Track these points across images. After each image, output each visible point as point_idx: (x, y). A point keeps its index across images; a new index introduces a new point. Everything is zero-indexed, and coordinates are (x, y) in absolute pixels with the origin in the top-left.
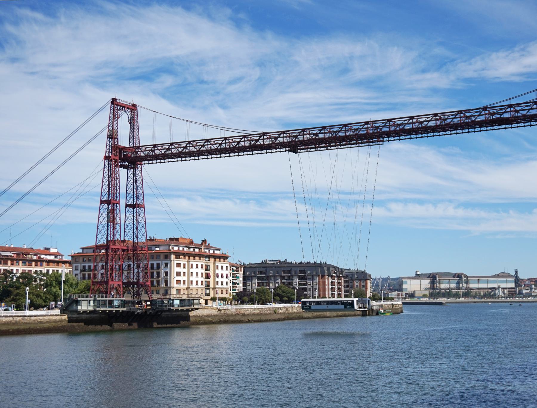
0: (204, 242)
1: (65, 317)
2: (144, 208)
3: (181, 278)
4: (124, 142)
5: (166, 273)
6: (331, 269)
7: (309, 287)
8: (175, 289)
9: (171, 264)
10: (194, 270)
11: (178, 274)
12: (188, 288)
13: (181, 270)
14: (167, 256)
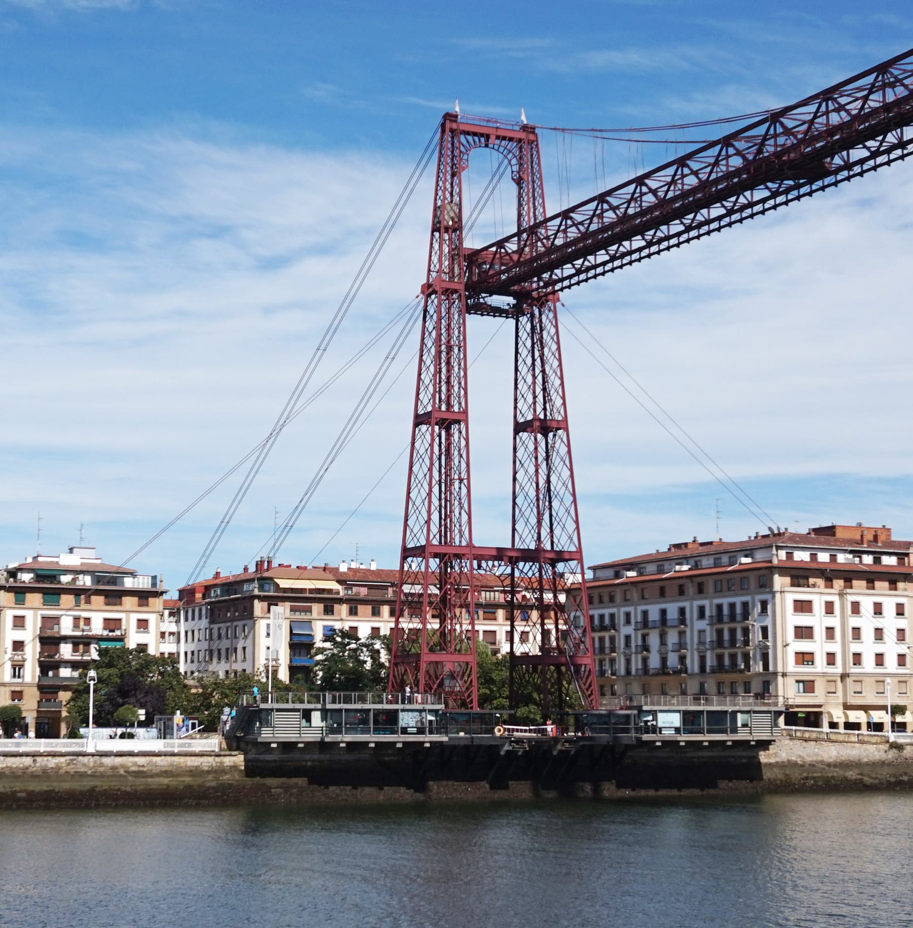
1: (239, 759)
2: (566, 430)
5: (764, 630)
8: (790, 681)
9: (774, 604)
10: (867, 622)
12: (844, 676)
14: (762, 578)
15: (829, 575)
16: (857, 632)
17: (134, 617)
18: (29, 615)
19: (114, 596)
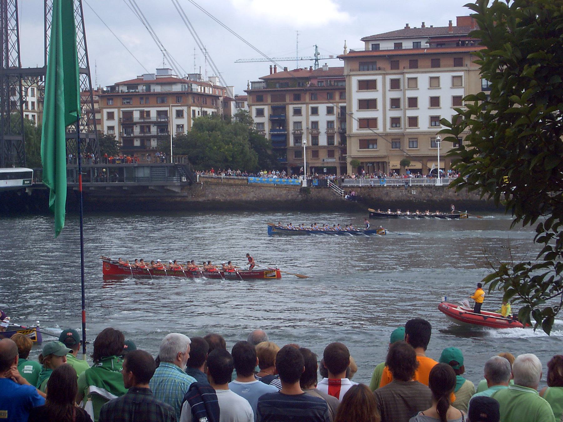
15: (394, 60)
16: (413, 102)
17: (174, 109)
18: (115, 111)
19: (162, 98)
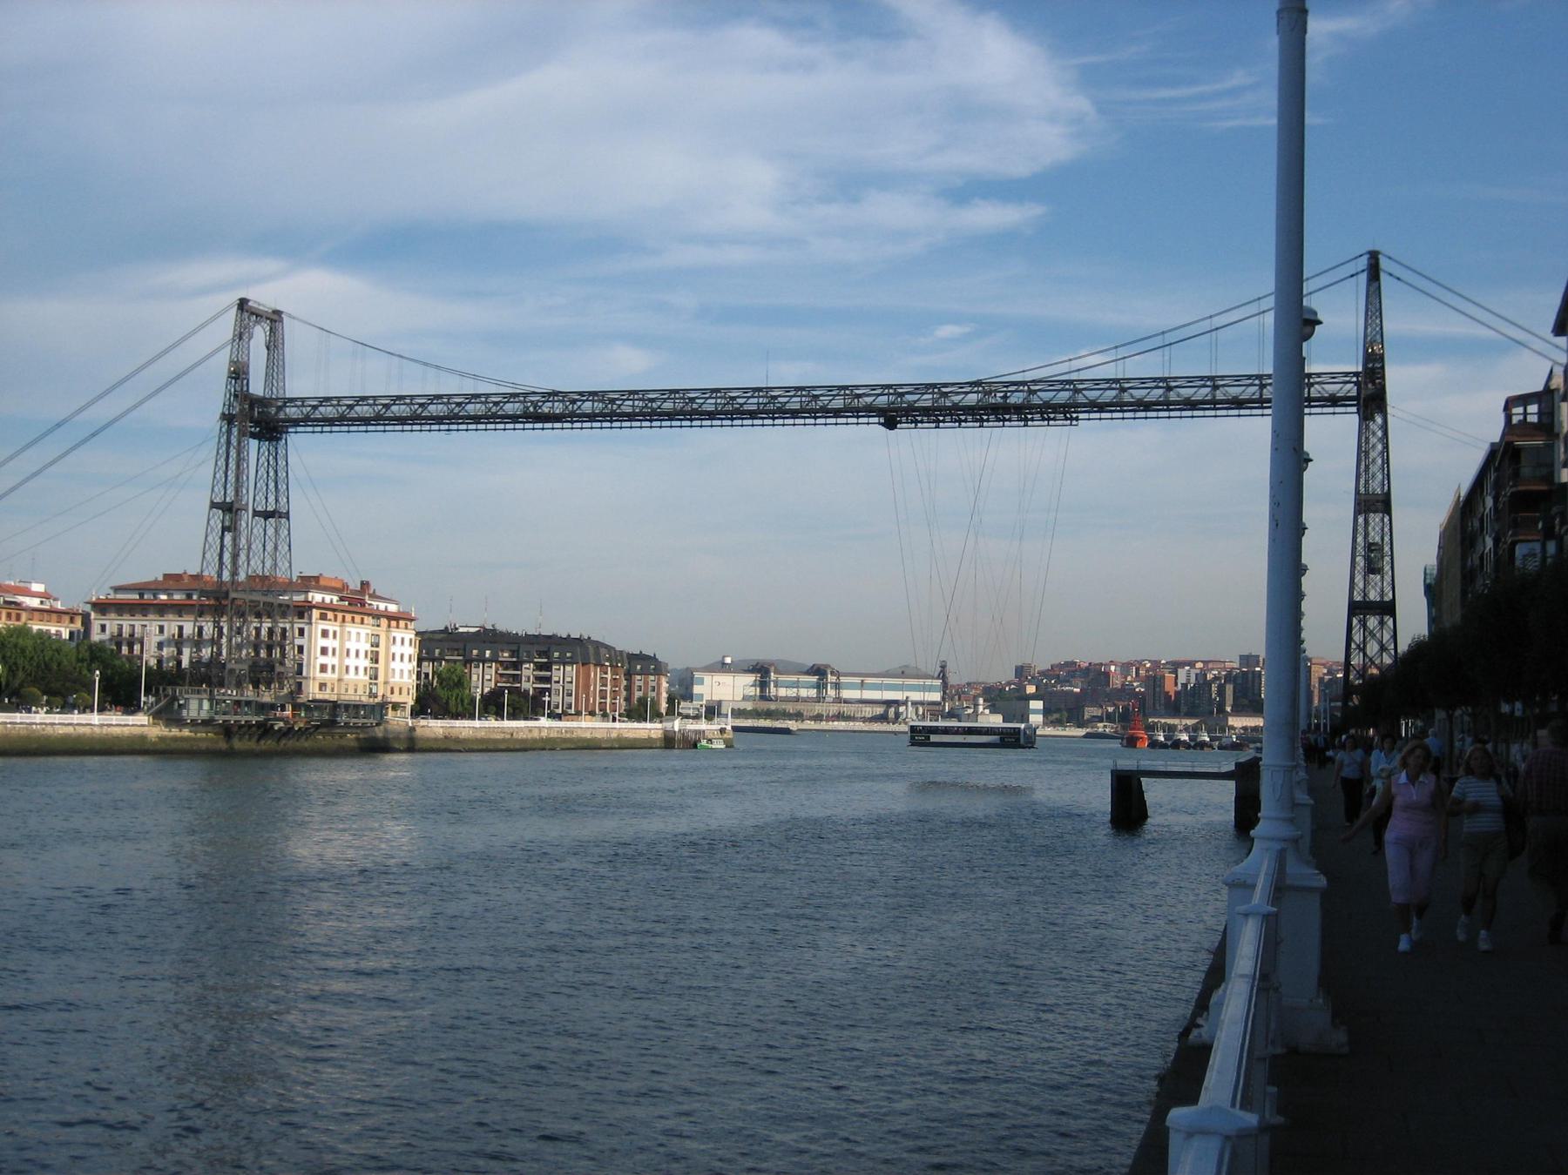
0: (365, 585)
3: (328, 660)
4: (257, 387)
5: (301, 649)
6: (603, 651)
7: (554, 686)
11: (324, 651)
13: (329, 643)
